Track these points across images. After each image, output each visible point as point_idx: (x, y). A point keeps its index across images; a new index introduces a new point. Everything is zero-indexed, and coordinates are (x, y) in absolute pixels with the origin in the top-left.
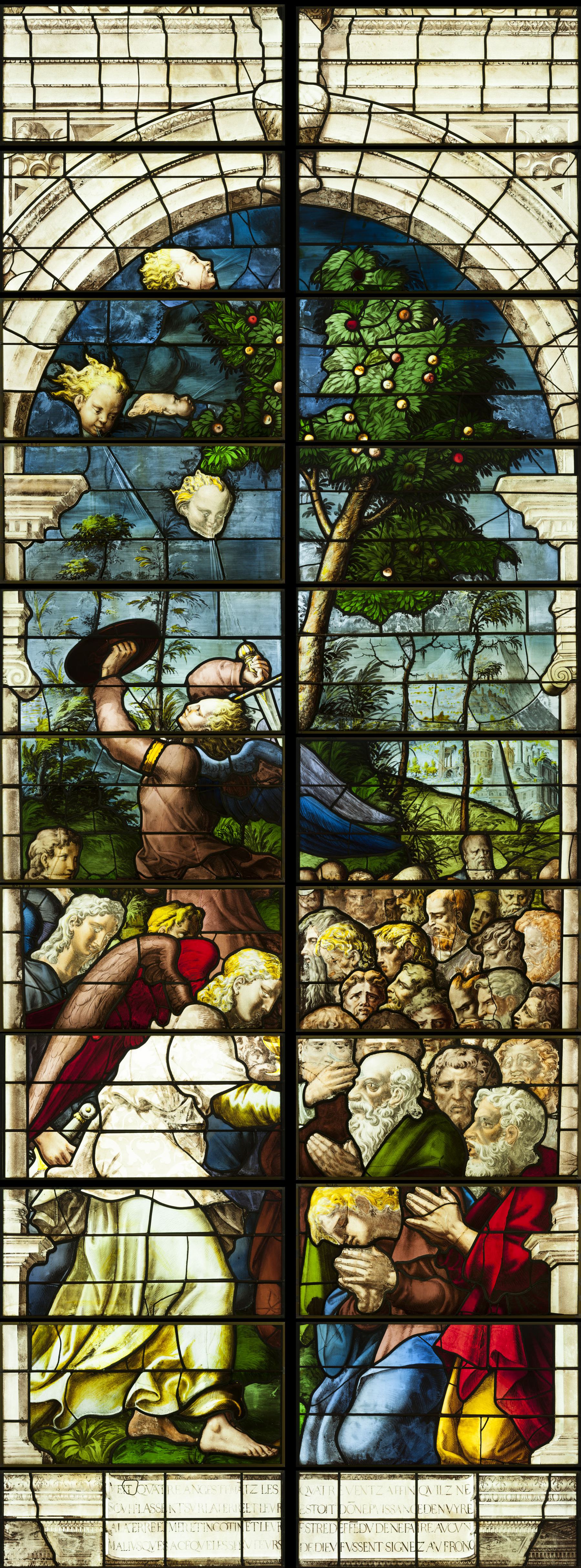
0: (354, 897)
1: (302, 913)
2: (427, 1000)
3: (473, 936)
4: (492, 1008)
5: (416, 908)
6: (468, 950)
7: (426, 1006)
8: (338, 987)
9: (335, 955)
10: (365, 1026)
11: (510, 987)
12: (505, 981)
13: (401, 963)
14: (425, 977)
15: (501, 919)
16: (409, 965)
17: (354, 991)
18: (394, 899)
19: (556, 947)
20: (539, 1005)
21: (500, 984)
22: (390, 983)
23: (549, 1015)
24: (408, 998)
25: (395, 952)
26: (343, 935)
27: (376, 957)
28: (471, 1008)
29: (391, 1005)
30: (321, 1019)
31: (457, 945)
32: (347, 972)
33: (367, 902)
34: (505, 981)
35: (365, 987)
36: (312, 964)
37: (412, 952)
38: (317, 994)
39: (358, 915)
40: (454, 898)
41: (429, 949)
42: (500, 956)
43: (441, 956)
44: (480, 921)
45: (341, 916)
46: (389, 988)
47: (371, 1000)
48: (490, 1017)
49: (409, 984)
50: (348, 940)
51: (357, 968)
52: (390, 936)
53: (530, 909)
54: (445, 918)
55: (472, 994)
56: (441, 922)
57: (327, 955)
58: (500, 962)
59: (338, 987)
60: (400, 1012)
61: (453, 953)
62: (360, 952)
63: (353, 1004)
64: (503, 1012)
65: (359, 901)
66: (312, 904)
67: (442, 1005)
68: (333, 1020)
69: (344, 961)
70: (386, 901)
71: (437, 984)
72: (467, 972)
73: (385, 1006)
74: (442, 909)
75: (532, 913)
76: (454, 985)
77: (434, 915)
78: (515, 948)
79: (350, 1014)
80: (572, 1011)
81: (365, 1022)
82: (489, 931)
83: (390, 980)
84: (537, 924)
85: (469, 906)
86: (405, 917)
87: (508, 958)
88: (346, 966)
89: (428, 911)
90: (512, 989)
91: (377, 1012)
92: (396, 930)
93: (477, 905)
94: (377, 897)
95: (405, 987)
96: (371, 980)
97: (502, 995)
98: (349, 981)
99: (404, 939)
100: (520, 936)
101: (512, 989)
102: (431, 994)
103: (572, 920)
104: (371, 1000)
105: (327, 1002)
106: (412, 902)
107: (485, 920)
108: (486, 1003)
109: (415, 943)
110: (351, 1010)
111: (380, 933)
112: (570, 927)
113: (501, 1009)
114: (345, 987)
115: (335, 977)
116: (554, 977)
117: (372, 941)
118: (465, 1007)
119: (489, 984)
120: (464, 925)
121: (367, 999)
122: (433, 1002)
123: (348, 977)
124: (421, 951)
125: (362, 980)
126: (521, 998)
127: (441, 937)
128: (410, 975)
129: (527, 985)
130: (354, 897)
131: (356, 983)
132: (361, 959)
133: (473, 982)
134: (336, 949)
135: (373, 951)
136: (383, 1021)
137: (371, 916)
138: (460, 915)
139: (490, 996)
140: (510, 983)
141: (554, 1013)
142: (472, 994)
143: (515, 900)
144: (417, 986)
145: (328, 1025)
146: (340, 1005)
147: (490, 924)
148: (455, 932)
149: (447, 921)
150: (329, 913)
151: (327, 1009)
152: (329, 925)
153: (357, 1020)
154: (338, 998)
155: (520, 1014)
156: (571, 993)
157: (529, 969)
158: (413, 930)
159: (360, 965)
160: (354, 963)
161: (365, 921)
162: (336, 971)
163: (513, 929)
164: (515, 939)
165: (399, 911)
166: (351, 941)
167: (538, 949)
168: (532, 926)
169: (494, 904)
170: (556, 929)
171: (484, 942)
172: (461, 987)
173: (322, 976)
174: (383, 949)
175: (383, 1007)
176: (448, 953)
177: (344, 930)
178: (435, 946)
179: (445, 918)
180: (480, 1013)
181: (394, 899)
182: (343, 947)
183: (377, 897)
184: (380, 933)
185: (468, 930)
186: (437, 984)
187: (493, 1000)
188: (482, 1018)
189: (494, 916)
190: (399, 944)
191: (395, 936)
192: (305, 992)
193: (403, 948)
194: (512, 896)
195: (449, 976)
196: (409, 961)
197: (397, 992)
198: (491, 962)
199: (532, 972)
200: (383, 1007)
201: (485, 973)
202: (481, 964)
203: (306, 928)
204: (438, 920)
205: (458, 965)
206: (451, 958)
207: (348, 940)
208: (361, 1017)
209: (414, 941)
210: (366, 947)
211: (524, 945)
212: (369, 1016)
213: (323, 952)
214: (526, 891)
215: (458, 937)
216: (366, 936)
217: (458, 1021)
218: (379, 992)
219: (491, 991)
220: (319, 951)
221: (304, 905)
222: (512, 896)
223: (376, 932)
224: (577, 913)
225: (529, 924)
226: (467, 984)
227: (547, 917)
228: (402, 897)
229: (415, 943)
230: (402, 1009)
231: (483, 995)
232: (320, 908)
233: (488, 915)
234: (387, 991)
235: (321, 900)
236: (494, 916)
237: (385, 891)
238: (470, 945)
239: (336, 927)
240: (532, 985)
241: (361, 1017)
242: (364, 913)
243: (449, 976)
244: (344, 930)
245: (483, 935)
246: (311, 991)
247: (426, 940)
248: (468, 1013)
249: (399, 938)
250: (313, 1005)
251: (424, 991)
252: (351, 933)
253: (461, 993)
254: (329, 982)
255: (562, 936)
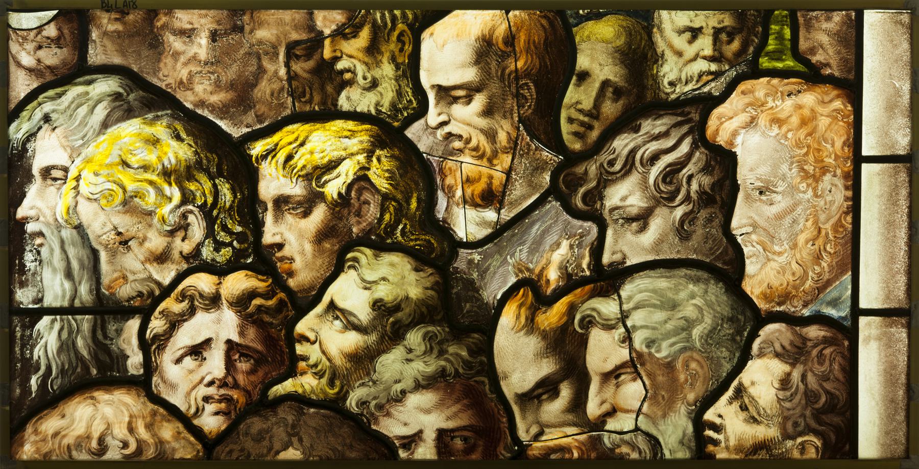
0: (188, 34)
1: (21, 85)
2: (421, 367)
3: (572, 159)
4: (632, 391)
5: (387, 70)
6: (554, 205)
7: (419, 386)
8: (134, 324)
9: (125, 223)
10: (221, 452)
11: (689, 324)
12: (674, 306)
13: (340, 246)
14: (415, 292)
15: (659, 106)
16: (364, 255)
17: (186, 336)
18: (317, 41)
19: (839, 196)
20: (785, 383)
21: (659, 316)
22: (302, 312)
23: (818, 415)
24: (362, 361)
25: (319, 213)
26: (151, 157)
27: (258, 227)
28: (566, 392)
29: (306, 383)
30: (79, 429)
31: (518, 189)
32: (166, 275)
33: (228, 52)
34: (674, 306)
35: (224, 325)
36: (51, 250)
37: (372, 211)
38: (67, 346)
39: (202, 93)
40: (510, 39)
41: (430, 203)
42: (657, 225)
43: (468, 223)
44: (594, 113)
45: (145, 97)
46: (301, 327)
47: (243, 366)
48: (624, 422)
49: (364, 314)
50: (166, 174)
51: (195, 263)
52: (302, 159)
53: (756, 73)
54: (479, 101)
55: (567, 346)
56: (467, 116)
57: (100, 223)
58: (658, 244)
59: (134, 324)
60: (334, 406)
61: (507, 215)
62: (207, 212)
63: (187, 381)
64: (668, 407)
65: (201, 46)
66: (52, 57)
67: (472, 381)
68: (120, 431)
69: (156, 242)
70: (291, 48)
71: (454, 315)
72: (553, 275)
73: (288, 386)
74: (470, 75)
75: (760, 86)
76: (508, 318)
77: (445, 93)
78: (705, 199)
79: (173, 411)
80: (890, 401)
81: (223, 436)
82: (622, 144)
83: (304, 302)
84: (777, 121)
85: (556, 63)
86: (353, 99)
87: (682, 231)
88: (161, 258)
89: (426, 80)
90: (697, 332)
91: (261, 404)
92: (322, 141)
93: (583, 62)
94: (262, 34)
95: (352, 325)
96: (241, 303)
97: (664, 352)
98: (172, 305)
99: (347, 171)
100: (723, 161)
101: (697, 332)
102: (435, 346)
103: (890, 108)
104: (243, 366)
105: (99, 372)
106: (373, 49)
107: (610, 109)
108: (612, 376)
109: (382, 184)
110: (177, 400)
111: (271, 152)
112: (884, 133)
113: (662, 395)
114: (157, 325)
115: (125, 291)
116: (832, 292)
117: (245, 175)
118: (546, 388)
119: (624, 317)
120: (542, 123)
121: (230, 364)
122: (442, 374)
123: (166, 291)
124: (402, 207)
125: (214, 301)
126: (725, 359)
127: (468, 164)
128: (368, 285)
129: (745, 320)
130: (188, 34)
131: (192, 311)
132: (210, 233)
133: (572, 309)
134: (129, 204)
135: (250, 208)
136: (280, 433)
137: (242, 97)
138: (530, 92)
139: (623, 354)
140: (689, 311)
141: (831, 406)
142: (567, 346)
143: (705, 44)
144: (389, 323)
145: (103, 447)
146: (143, 384)
147: (626, 122)
148: (514, 147)
149: (488, 112)
150: (105, 86)
151: (101, 396)
152: (105, 125)
153: (197, 432)
154: (135, 361)
155: (723, 411)
156: (888, 343)
157: (750, 268)
158: (378, 143)
159: (207, 253)
160: (187, 247)
161: (223, 111)
162: (130, 273)
163: (701, 139)
164: (706, 169)
165: (330, 78)
166: (179, 175)
167: (781, 203)
168: (761, 129)
169: (639, 57)
170: (838, 139)
171: (606, 180)
172: (530, 326)
173: (84, 290)
174: (281, 202)
175: (279, 389)
176: (490, 215)
177: (154, 142)
178: (449, 192)
179: (479, 101)
180: (593, 408)
181: (317, 41)
182: (151, 197)
183: (262, 34)
184: (271, 152)
185: (555, 143)
186: (454, 315)
187: (634, 365)
188: (599, 424)
189: (639, 94)
190: (333, 187)
191: (320, 159)
192: (29, 342)
193: (344, 200)
194: (695, 33)
195: (493, 291)
196: (364, 241)
197: (327, 339)
198: (628, 246)
199: (761, 276)
200: (279, 389)
201: (608, 278)
202: (597, 250)
203: (31, 136)
204: (459, 110)
205: (521, 254)
206: (499, 232)
207: (166, 174)
208: (211, 422)
209: (379, 177)
210: (227, 195)
211: (735, 188)
212: (237, 416)
213: (87, 213)
214: (740, 16)
215: (522, 165)
216: (228, 158)
217: (523, 436)
218: (268, 340)
219: (628, 339)
220: (73, 210)
221: (27, 60)
222: (695, 33)
223: (258, 148)
224: (906, 87)
225: (752, 123)
226: (552, 317)
227: (809, 99)
228: (340, 34)
229: (382, 184)
230: (343, 396)
231: (604, 350)
232: (77, 70)
233: (618, 93)
234: (292, 339)
235: (81, 43)
236: (639, 94)
237: (287, 16)
238: (561, 190)
239: (130, 130)
240: (761, 319)
241: (211, 422)
242: (218, 86)
243: (493, 291)
244: (154, 142)
245: (604, 157)
246: (48, 336)
247: (419, 173)
248: (554, 408)
249: (332, 165)
250: (55, 384)
251: (414, 338)
252: (177, 151)
253: (532, 343)
254: (107, 310)
255: (858, 159)
